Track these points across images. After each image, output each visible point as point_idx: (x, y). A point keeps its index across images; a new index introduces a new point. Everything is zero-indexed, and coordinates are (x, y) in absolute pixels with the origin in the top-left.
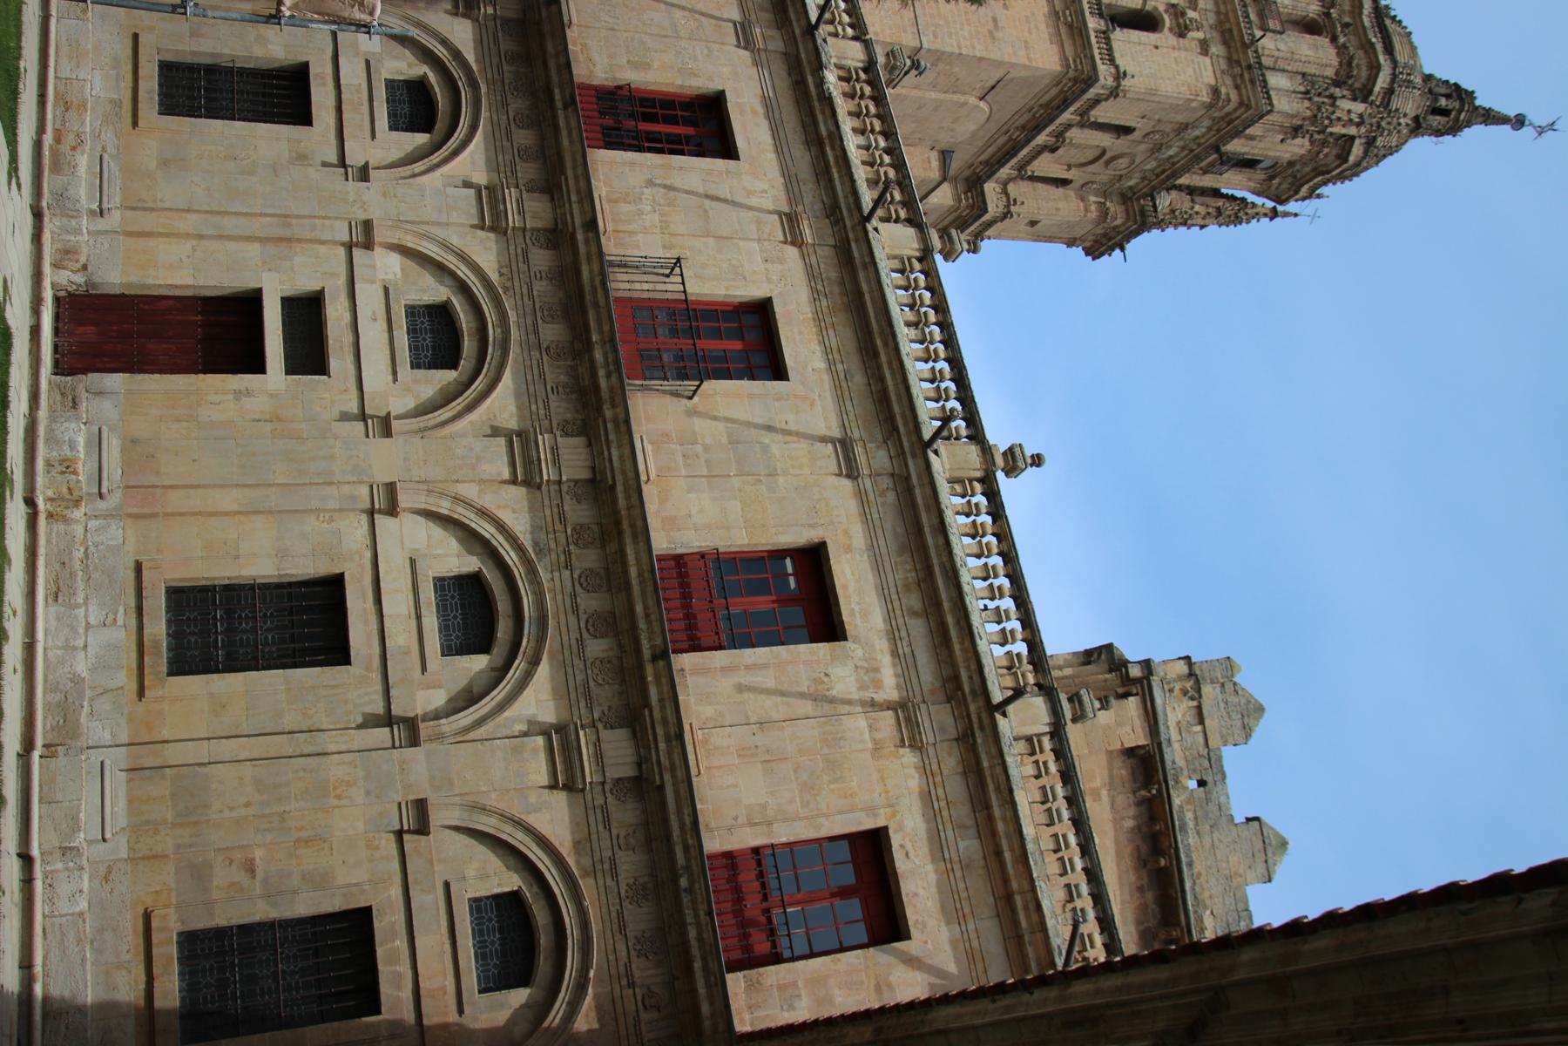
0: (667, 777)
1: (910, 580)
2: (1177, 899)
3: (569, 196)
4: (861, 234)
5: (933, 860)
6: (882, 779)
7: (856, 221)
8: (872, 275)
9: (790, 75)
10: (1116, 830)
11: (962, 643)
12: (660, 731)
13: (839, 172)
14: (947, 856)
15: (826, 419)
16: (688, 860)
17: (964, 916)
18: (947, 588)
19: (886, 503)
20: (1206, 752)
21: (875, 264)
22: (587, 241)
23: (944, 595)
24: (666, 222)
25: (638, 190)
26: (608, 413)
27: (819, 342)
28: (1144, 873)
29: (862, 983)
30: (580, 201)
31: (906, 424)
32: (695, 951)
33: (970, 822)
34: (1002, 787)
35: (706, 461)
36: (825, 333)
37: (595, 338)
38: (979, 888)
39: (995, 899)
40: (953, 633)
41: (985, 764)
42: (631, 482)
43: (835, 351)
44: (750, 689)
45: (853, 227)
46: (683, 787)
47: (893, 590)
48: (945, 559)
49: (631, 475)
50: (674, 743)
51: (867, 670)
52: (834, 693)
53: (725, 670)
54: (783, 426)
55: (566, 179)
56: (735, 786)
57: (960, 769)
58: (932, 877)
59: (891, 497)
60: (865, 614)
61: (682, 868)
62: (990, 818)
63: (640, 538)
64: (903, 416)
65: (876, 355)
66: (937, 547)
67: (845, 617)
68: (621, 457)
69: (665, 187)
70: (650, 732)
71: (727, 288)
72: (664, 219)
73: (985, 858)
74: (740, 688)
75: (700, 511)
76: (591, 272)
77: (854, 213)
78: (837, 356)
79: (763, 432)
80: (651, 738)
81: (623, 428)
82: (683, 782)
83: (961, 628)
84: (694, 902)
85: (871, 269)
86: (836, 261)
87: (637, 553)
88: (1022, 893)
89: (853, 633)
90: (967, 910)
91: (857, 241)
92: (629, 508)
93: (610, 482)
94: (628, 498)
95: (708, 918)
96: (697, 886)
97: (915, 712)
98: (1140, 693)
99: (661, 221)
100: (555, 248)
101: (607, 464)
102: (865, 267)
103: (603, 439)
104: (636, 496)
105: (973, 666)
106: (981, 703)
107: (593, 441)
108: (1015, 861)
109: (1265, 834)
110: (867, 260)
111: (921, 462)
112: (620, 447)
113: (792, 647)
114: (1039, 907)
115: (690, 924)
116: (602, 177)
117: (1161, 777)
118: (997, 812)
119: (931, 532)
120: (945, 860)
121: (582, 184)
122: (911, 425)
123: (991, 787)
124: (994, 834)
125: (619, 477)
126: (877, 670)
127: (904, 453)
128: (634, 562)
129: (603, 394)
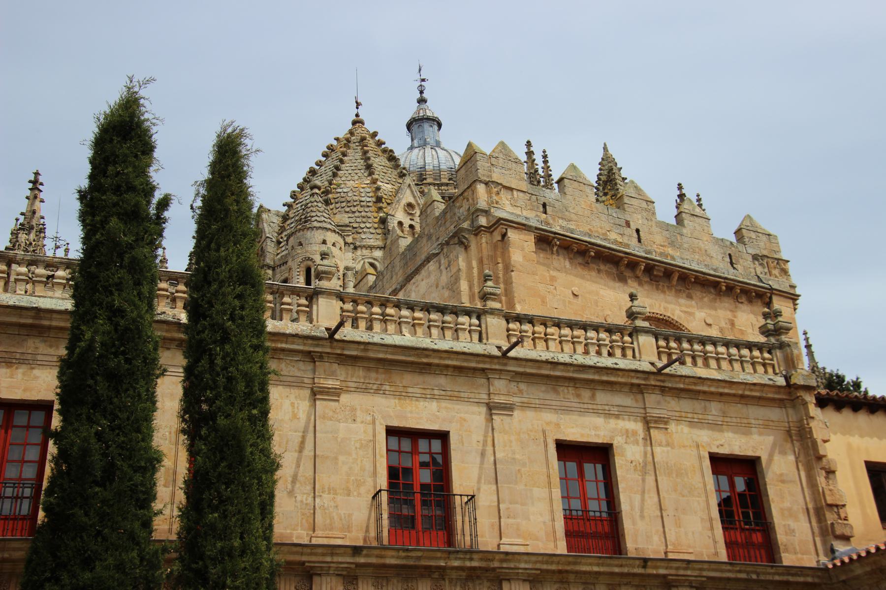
0: (705, 573)
1: (573, 392)
2: (611, 253)
3: (327, 562)
4: (340, 344)
5: (722, 431)
6: (684, 447)
7: (329, 344)
8: (375, 348)
9: (168, 349)
10: (570, 274)
11: (618, 376)
12: (681, 572)
13: (282, 342)
14: (720, 423)
15: (473, 413)
16: (745, 572)
17: (748, 424)
18: (587, 373)
19: (536, 393)
20: (528, 195)
21: (369, 343)
22: (367, 556)
23: (591, 377)
24: (329, 489)
25: (299, 505)
26: (496, 564)
27: (417, 400)
28: (592, 265)
29: (780, 489)
30: (332, 555)
31: (484, 362)
32: (785, 578)
33: (703, 403)
34: (695, 382)
35: (511, 503)
36: (410, 395)
37: (442, 564)
38: (736, 410)
39: (739, 403)
40: (612, 379)
41: (682, 386)
42: (545, 559)
43: (424, 392)
44: (642, 511)
45: (331, 347)
46: (713, 566)
47: (582, 406)
48: (572, 369)
49: (540, 558)
50: (690, 566)
51: (627, 437)
52: (641, 461)
53: (634, 523)
54: (481, 444)
55: (309, 562)
56: (693, 533)
57: (676, 399)
58: (730, 435)
59: (523, 386)
60: (596, 428)
61: (748, 575)
62: (704, 392)
63: (579, 560)
64: (478, 362)
65: (429, 364)
66: (563, 371)
67: (600, 441)
68: (526, 562)
69: (294, 482)
70: (680, 578)
71: (382, 456)
72: (326, 489)
73: (720, 402)
74: (642, 517)
75: (541, 515)
76: (393, 557)
77: (320, 343)
78: (428, 392)
79: (486, 459)
80: (683, 578)
81: (510, 557)
82: (710, 566)
83: (611, 374)
84: (764, 573)
85: (370, 347)
86: (350, 368)
87: (586, 564)
88: (744, 390)
89: (609, 439)
90: (745, 421)
91: (343, 349)
92: (558, 563)
93: (539, 572)
94: (552, 563)
95: (774, 568)
96: (758, 570)
97: (653, 417)
98: (506, 227)
99: (329, 493)
100: (357, 579)
101: (528, 571)
102: (366, 350)
103: (511, 571)
104: (554, 558)
105: (633, 374)
106: (652, 377)
107: (508, 577)
108: (730, 388)
109: (571, 178)
110: (362, 347)
111: (511, 362)
112: (519, 561)
113: (619, 479)
114: (754, 384)
115: (773, 578)
116: (288, 531)
117: (553, 235)
118: (705, 388)
119: (553, 371)
120: (722, 425)
121: (320, 551)
122: (488, 360)
123: (693, 387)
124: (712, 393)
125: (538, 566)
126: (627, 431)
127: (501, 370)
128: (590, 567)
129: (483, 566)
